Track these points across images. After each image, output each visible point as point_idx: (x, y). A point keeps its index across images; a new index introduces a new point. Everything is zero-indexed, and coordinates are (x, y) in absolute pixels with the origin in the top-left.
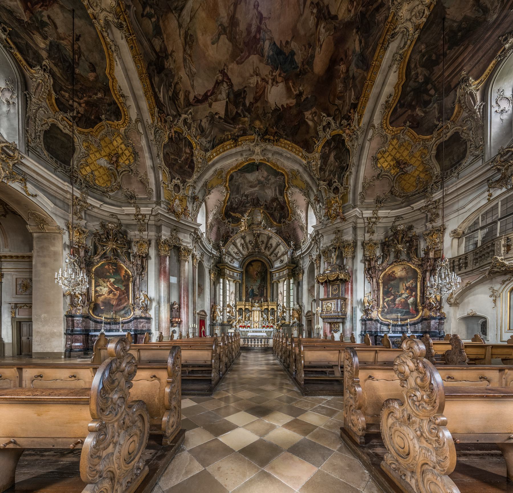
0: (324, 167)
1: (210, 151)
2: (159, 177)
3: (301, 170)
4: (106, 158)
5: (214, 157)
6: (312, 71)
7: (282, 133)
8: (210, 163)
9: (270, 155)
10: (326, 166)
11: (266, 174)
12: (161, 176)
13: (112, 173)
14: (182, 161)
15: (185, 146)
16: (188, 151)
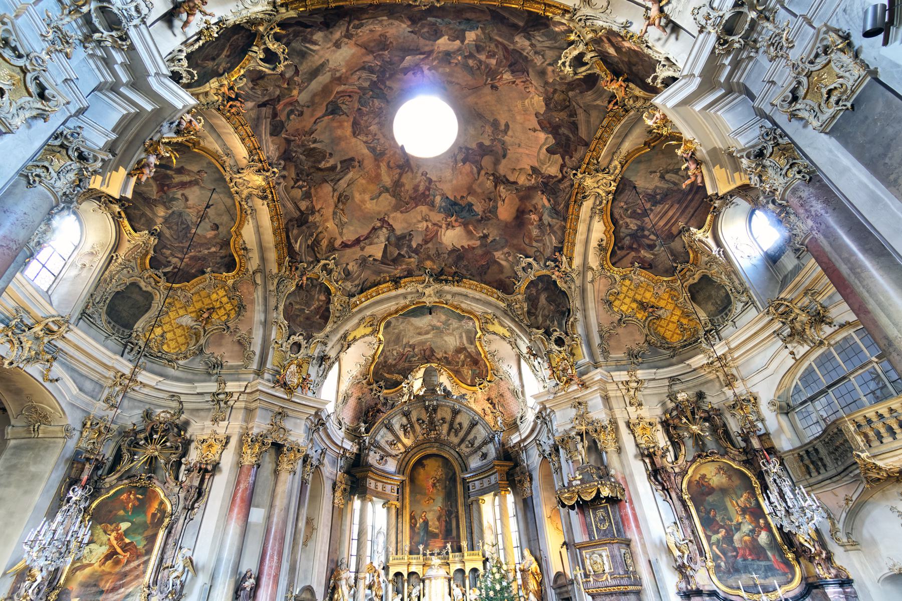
0: (533, 311)
1: (357, 296)
2: (270, 335)
3: (498, 313)
4: (193, 315)
5: (362, 302)
6: (497, 217)
7: (465, 272)
8: (354, 310)
9: (449, 297)
10: (536, 309)
11: (443, 318)
12: (274, 333)
13: (195, 334)
14: (311, 311)
15: (320, 292)
16: (323, 298)
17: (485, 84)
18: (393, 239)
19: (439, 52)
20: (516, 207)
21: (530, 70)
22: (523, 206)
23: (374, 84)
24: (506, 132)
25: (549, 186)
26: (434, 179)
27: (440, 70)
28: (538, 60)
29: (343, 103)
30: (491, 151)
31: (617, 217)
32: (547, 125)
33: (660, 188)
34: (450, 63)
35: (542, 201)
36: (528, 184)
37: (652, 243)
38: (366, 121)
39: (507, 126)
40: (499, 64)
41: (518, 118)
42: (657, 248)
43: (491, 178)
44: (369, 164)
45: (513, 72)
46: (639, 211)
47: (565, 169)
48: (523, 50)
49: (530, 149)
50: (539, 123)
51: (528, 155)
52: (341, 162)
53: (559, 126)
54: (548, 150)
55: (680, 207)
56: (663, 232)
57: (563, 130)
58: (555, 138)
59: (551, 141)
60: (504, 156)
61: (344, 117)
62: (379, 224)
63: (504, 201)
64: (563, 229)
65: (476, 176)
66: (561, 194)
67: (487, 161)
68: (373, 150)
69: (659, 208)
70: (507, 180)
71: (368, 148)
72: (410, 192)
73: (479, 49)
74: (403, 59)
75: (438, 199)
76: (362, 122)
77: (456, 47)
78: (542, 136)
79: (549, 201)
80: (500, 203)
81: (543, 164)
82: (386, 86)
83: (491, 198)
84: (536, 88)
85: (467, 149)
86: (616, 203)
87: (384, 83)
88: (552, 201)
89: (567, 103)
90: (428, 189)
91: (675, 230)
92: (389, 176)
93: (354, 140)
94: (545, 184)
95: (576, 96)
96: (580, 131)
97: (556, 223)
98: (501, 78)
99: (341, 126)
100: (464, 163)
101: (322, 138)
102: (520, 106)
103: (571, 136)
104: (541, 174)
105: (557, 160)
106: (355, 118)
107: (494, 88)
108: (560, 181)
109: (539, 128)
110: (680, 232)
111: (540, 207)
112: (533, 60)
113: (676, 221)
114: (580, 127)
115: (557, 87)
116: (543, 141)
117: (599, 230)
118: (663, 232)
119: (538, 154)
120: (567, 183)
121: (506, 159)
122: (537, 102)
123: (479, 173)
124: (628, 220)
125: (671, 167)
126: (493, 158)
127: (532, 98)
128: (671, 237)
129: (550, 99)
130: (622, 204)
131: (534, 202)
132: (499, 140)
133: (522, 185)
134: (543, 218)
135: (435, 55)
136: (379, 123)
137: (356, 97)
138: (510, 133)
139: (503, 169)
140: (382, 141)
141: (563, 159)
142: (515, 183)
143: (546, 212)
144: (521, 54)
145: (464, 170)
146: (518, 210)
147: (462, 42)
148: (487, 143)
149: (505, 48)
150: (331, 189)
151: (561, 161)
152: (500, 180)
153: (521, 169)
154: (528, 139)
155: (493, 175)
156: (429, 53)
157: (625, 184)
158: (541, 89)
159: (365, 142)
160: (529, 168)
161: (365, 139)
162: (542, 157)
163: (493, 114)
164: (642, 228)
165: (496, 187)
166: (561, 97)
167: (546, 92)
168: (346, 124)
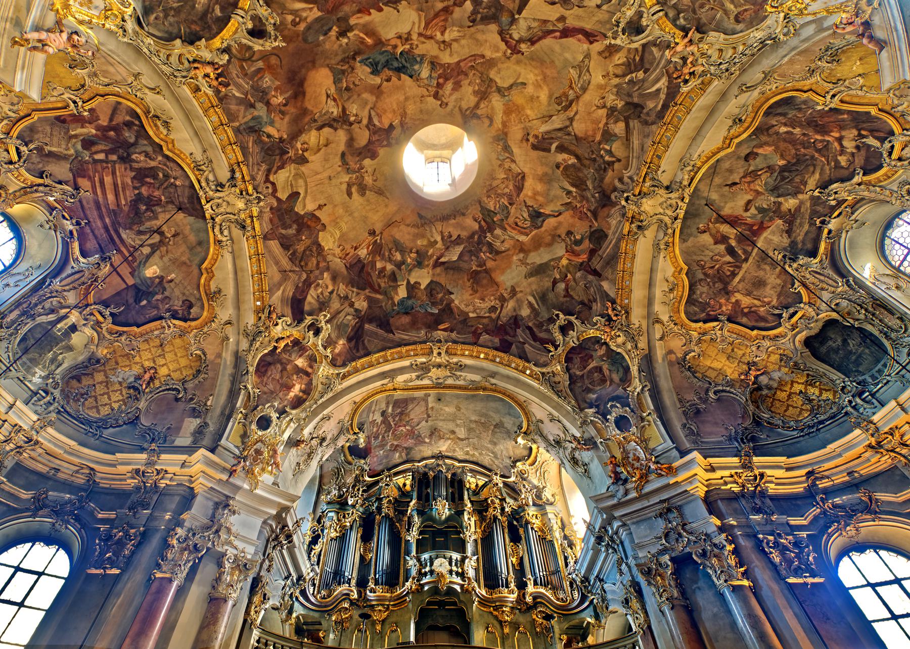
17: (381, 233)
18: (505, 19)
19: (428, 266)
20: (307, 98)
21: (345, 272)
22: (299, 104)
23: (491, 229)
24: (349, 186)
25: (276, 154)
26: (431, 100)
27: (425, 243)
28: (342, 289)
29: (526, 220)
30: (360, 153)
31: (171, 164)
32: (309, 224)
33: (150, 219)
34: (417, 252)
35: (276, 130)
36: (304, 137)
37: (94, 149)
38: (507, 187)
39: (349, 194)
40: (373, 263)
41: (341, 211)
42: (79, 147)
43: (352, 119)
44: (516, 133)
45: (359, 260)
46: (148, 180)
47: (270, 190)
48: (358, 294)
49: (317, 180)
50: (318, 219)
51: (317, 173)
52: (549, 151)
53: (299, 231)
54: (298, 194)
55: (108, 209)
56: (96, 171)
57: (291, 231)
58: (297, 213)
59: (299, 209)
60: (343, 155)
61: (529, 203)
62: (523, 47)
63: (328, 96)
64: (232, 117)
65: (373, 113)
66: (258, 158)
67: (363, 137)
68: (507, 148)
69: (130, 194)
70: (331, 126)
71: (511, 153)
72: (466, 82)
73: (393, 277)
74: (461, 255)
75: (425, 73)
76: (511, 187)
77: (413, 274)
78: (311, 206)
79: (269, 136)
80: (333, 90)
81: (296, 175)
82: (479, 223)
83: (346, 92)
84: (334, 255)
85: (389, 145)
86: (187, 183)
87: (481, 227)
88: (265, 139)
89: (303, 264)
90: (439, 86)
91: (84, 183)
92: (493, 109)
93: (526, 170)
94: (284, 152)
95: (300, 278)
96: (279, 246)
97: (245, 117)
98: (368, 248)
99: (536, 193)
100: (391, 125)
101: (559, 192)
102: (343, 225)
103: (283, 232)
104: (294, 161)
105: (283, 192)
106: (518, 195)
107: (372, 233)
108: (269, 171)
109: (317, 213)
110: (77, 188)
111: (277, 119)
112: (347, 286)
113: (95, 192)
114: (281, 250)
115: (317, 272)
116: (307, 201)
117: (184, 142)
118: (96, 171)
119: (306, 185)
120: (260, 177)
121: (340, 153)
122: (328, 241)
123: (370, 118)
124: (153, 164)
125: (164, 249)
126: (356, 145)
127: (334, 242)
128: (79, 171)
129: (319, 254)
130: (178, 183)
131: (287, 119)
132: (354, 172)
133: (310, 130)
134: (265, 108)
135: (431, 262)
136: (494, 179)
137: (511, 220)
138: (344, 187)
139: (341, 136)
140: (494, 156)
141: (278, 200)
142: (319, 128)
143: (265, 117)
144: (358, 288)
145: (390, 116)
146: (304, 94)
147: (408, 282)
148: (367, 162)
149: (372, 287)
150: (575, 124)
151: (279, 195)
152: (342, 120)
153: (319, 150)
154: (322, 192)
155: (351, 124)
156: (437, 264)
157: (195, 210)
158: (330, 258)
159: (513, 161)
160: (310, 158)
161: (513, 166)
162: (301, 182)
163: (368, 201)
164: (125, 159)
165: (344, 110)
166: (310, 264)
167: (325, 260)
168: (530, 194)
